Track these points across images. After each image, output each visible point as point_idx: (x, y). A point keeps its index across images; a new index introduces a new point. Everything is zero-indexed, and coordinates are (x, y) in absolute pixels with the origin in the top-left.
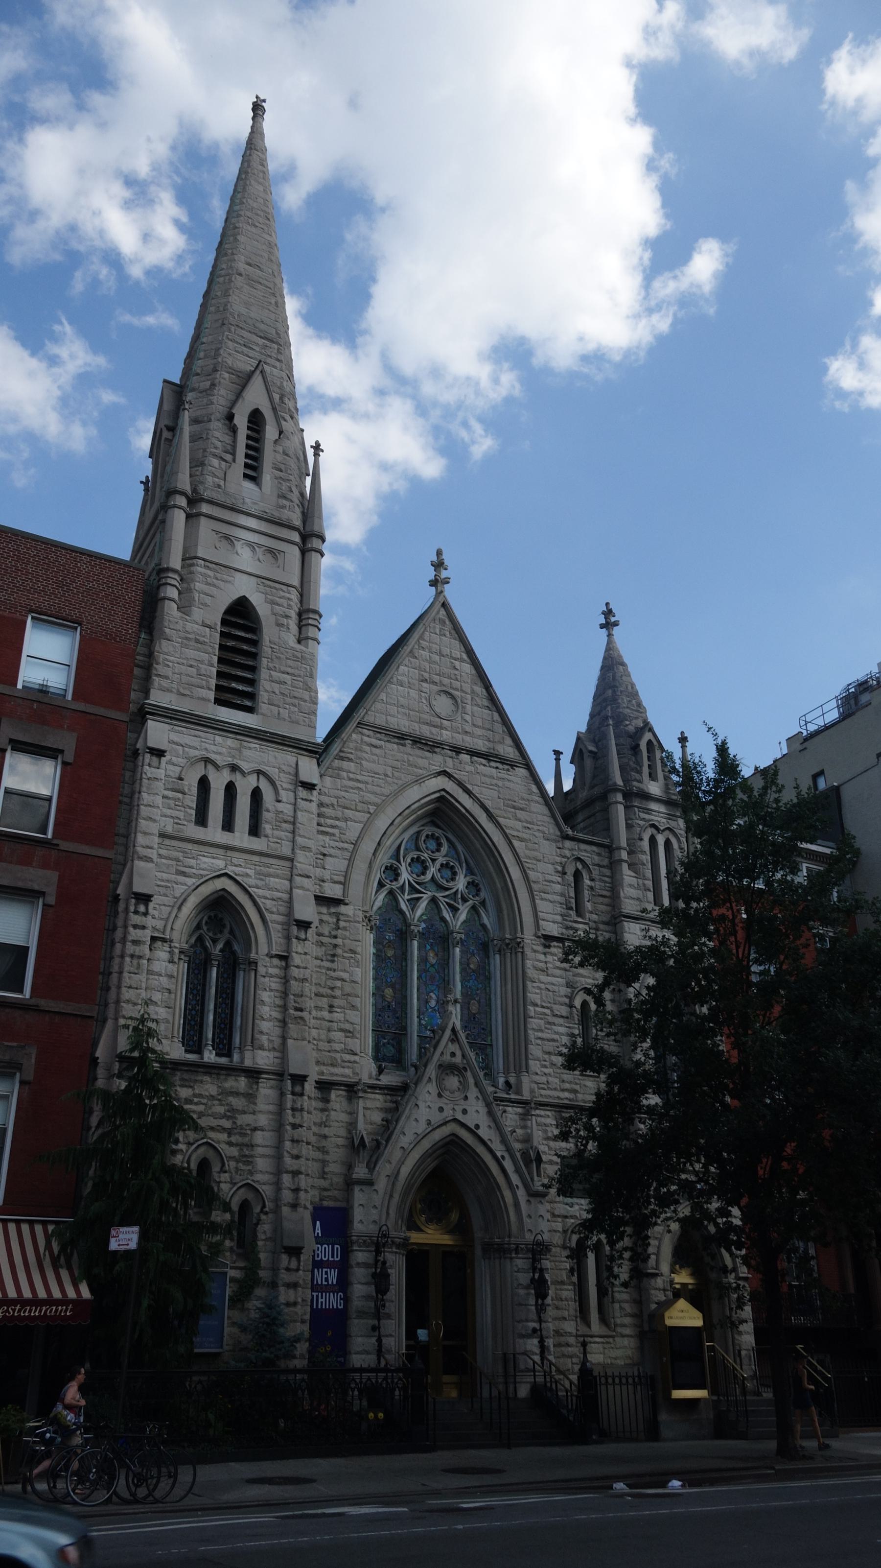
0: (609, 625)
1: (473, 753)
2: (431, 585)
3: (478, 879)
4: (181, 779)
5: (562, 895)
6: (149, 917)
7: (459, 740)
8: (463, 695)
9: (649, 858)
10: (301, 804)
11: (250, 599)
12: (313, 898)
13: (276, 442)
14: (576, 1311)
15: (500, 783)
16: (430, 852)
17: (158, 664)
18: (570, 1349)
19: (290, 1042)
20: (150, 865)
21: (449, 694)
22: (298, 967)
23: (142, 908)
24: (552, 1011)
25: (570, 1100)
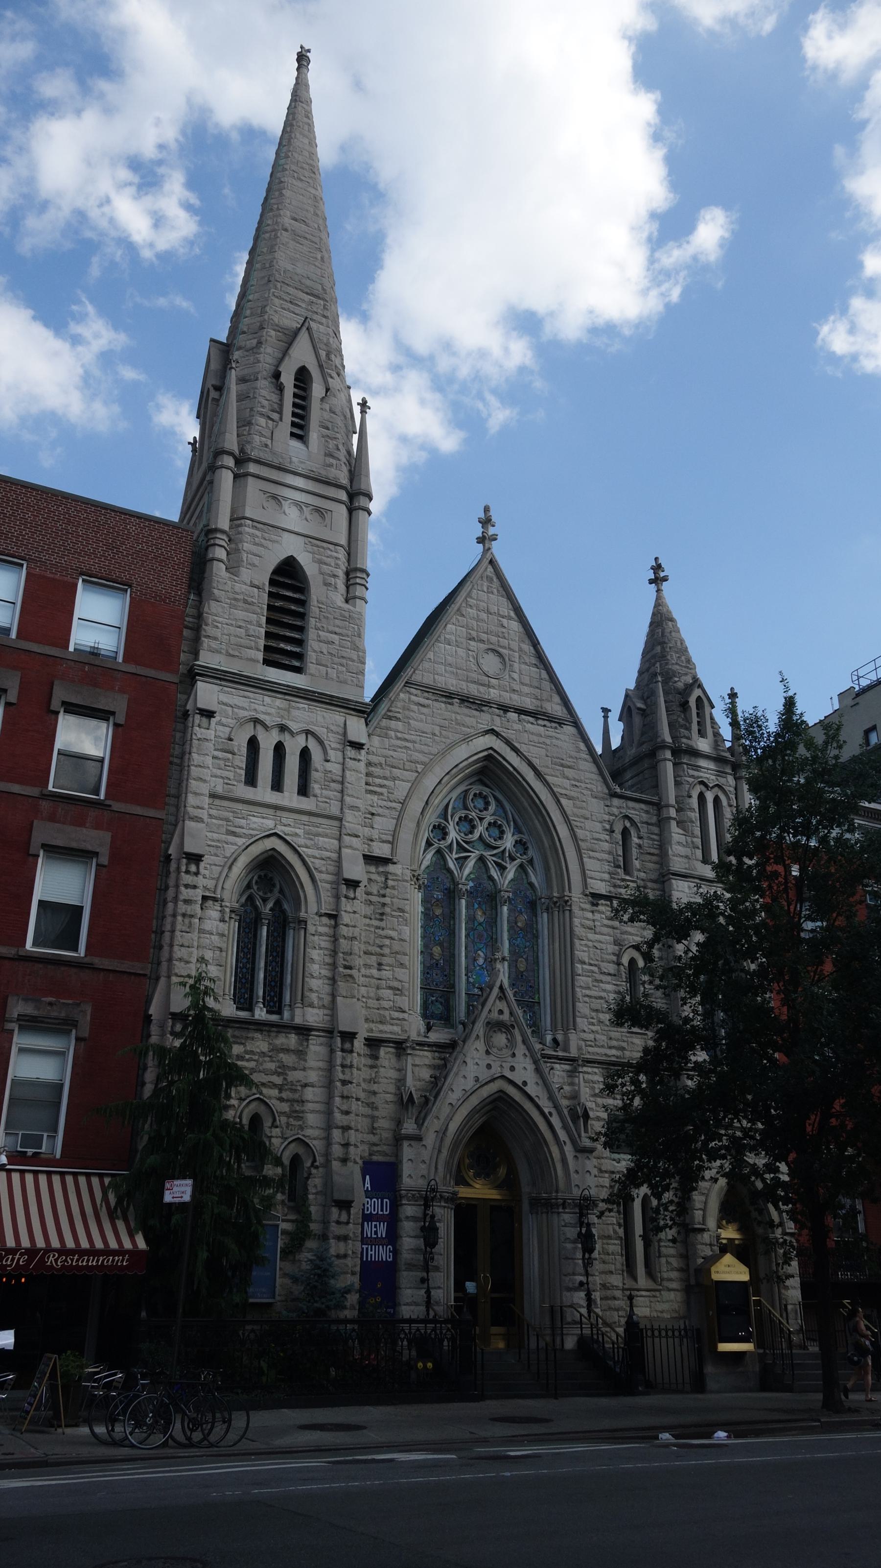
0: (658, 580)
1: (521, 711)
2: (478, 542)
3: (525, 838)
4: (231, 740)
5: (610, 853)
6: (200, 877)
7: (507, 698)
8: (511, 653)
9: (698, 815)
10: (350, 763)
11: (298, 558)
12: (361, 860)
13: (322, 399)
14: (623, 1265)
15: (548, 741)
16: (477, 811)
17: (207, 625)
19: (339, 999)
20: (201, 825)
21: (497, 652)
22: (347, 925)
23: (193, 868)
24: (599, 968)
25: (617, 1057)
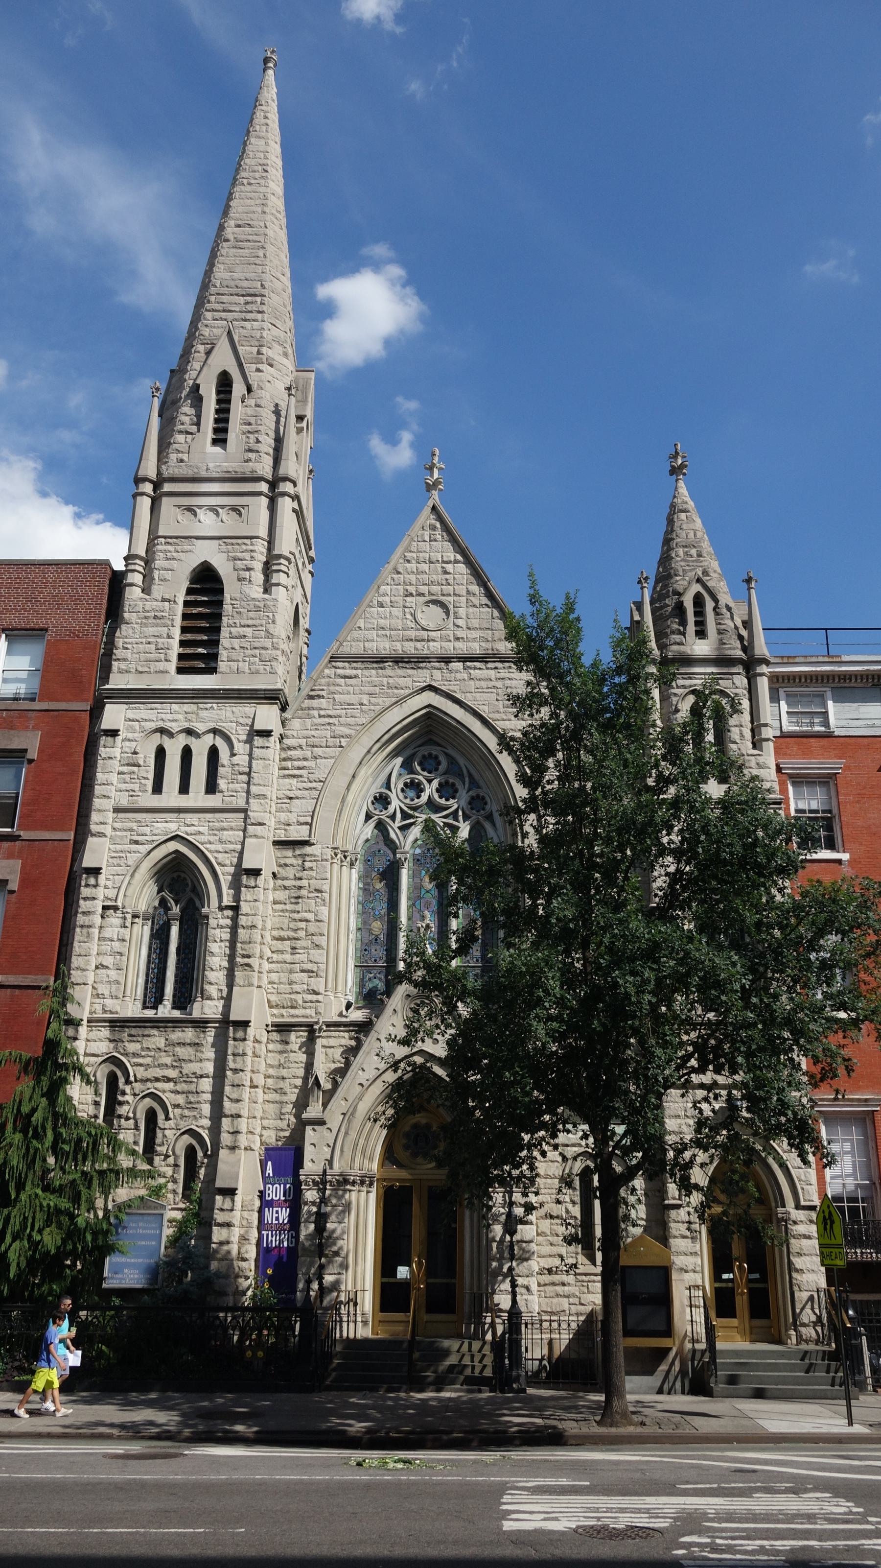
4: (135, 753)
7: (451, 648)
8: (456, 598)
10: (257, 752)
18: (566, 1288)
20: (104, 839)
22: (247, 915)
23: (92, 881)
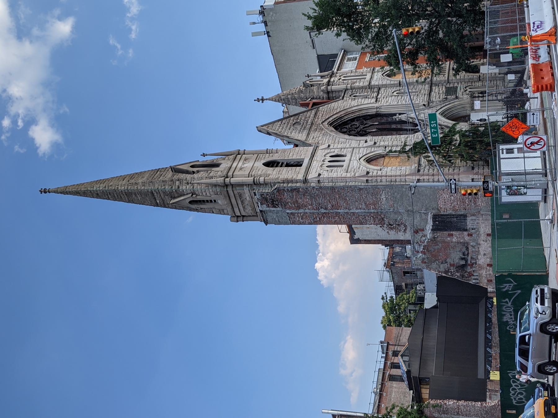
5: (362, 99)
